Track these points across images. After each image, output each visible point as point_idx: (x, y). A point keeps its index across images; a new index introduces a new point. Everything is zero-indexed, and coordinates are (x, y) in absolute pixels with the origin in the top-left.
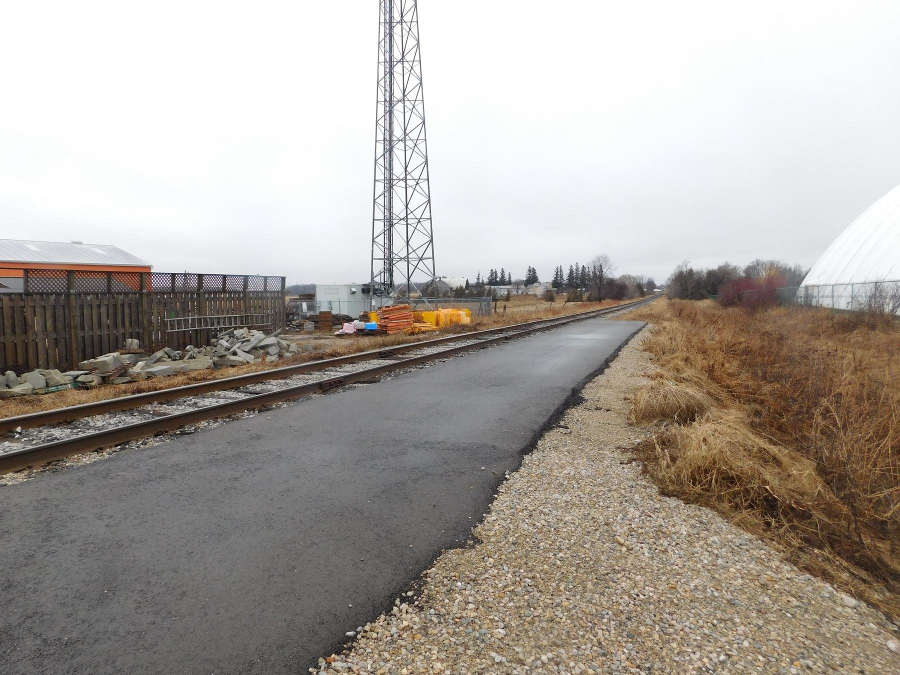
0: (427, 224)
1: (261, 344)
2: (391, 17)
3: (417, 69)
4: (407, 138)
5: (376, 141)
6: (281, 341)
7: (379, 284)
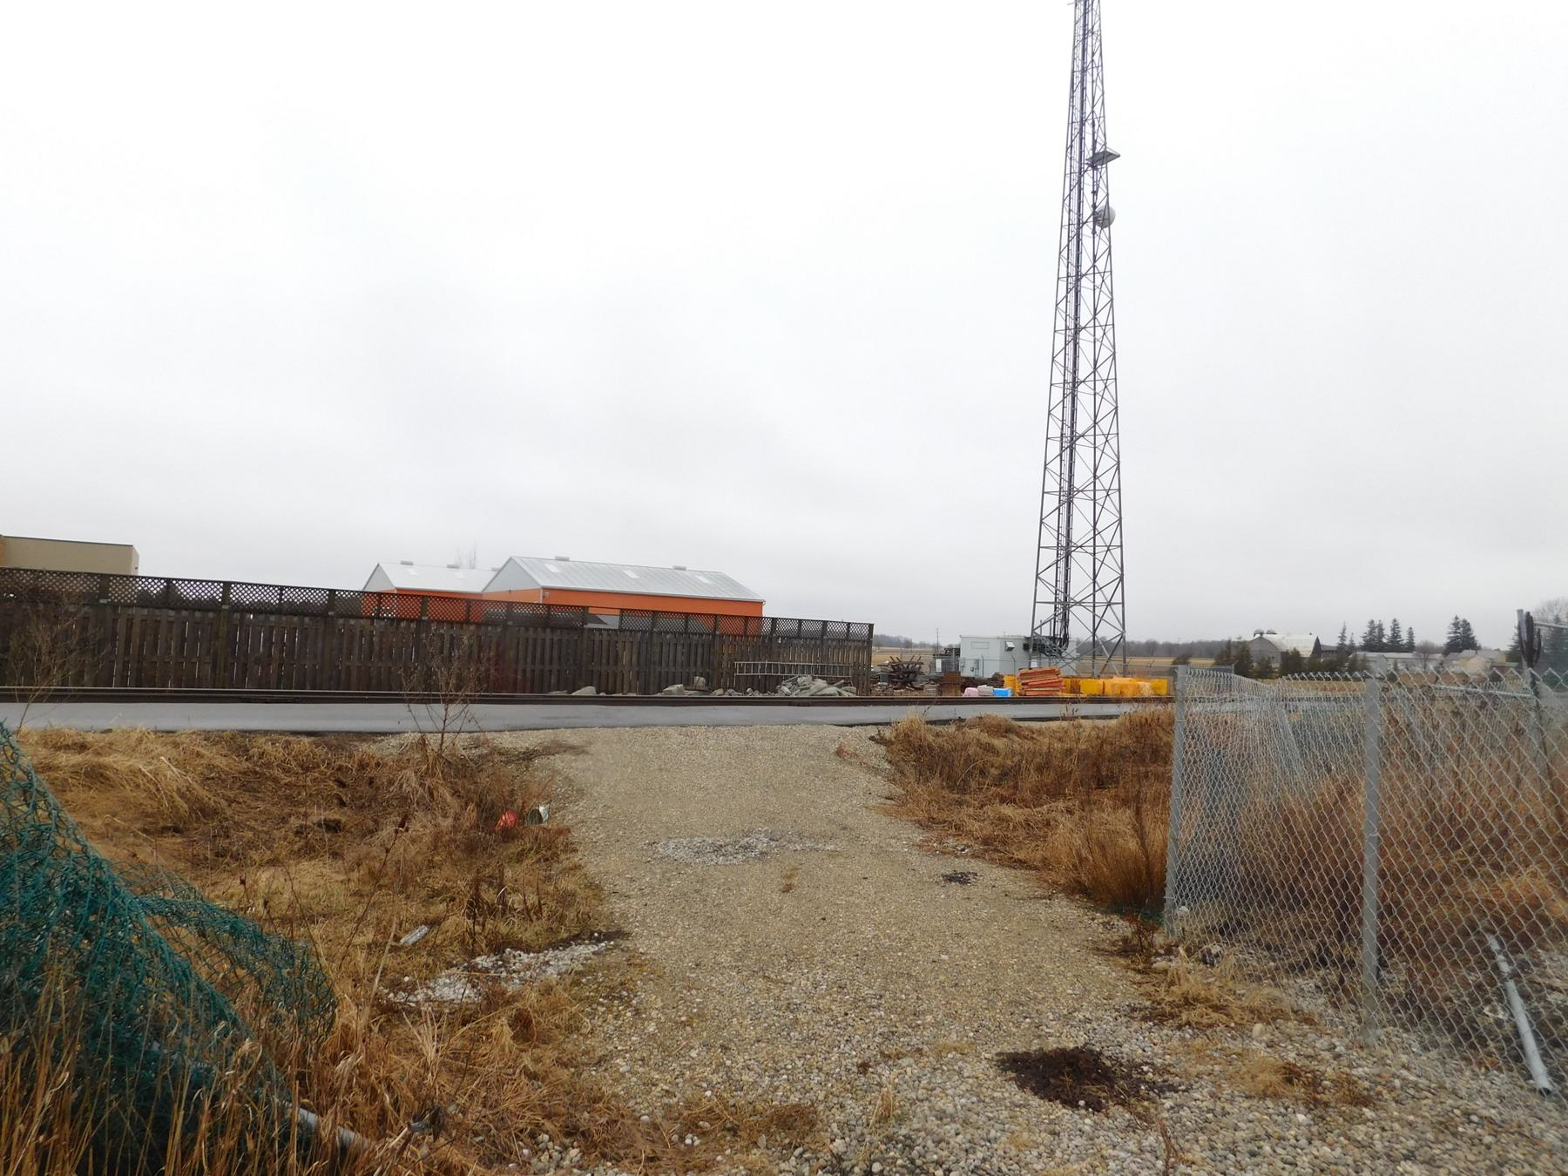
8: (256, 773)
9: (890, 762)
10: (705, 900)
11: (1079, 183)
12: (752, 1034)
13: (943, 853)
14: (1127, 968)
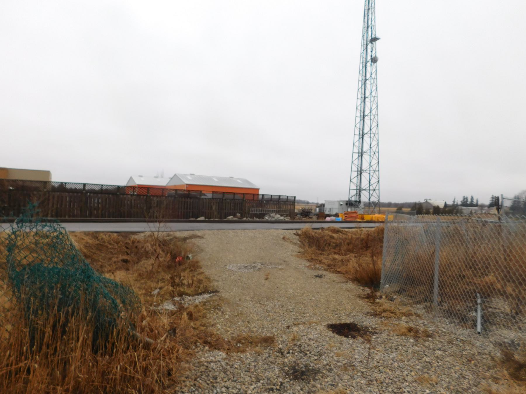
0: (377, 173)
8: (101, 244)
9: (300, 241)
10: (242, 282)
11: (366, 48)
12: (256, 318)
13: (315, 269)
14: (368, 302)
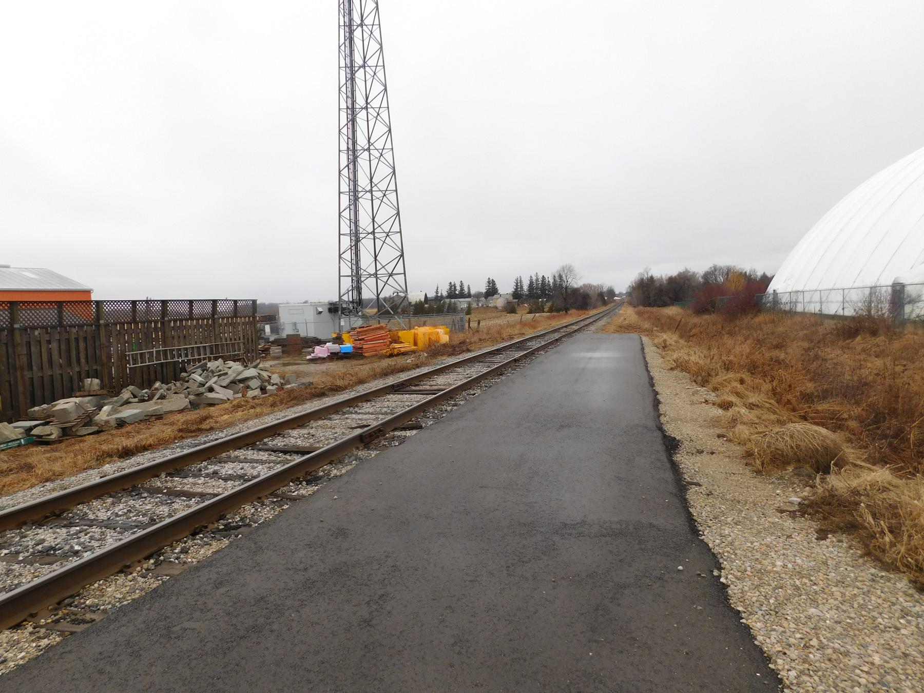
1: (240, 377)
2: (351, 20)
3: (380, 74)
4: (372, 147)
5: (340, 151)
6: (261, 372)
7: (346, 302)
